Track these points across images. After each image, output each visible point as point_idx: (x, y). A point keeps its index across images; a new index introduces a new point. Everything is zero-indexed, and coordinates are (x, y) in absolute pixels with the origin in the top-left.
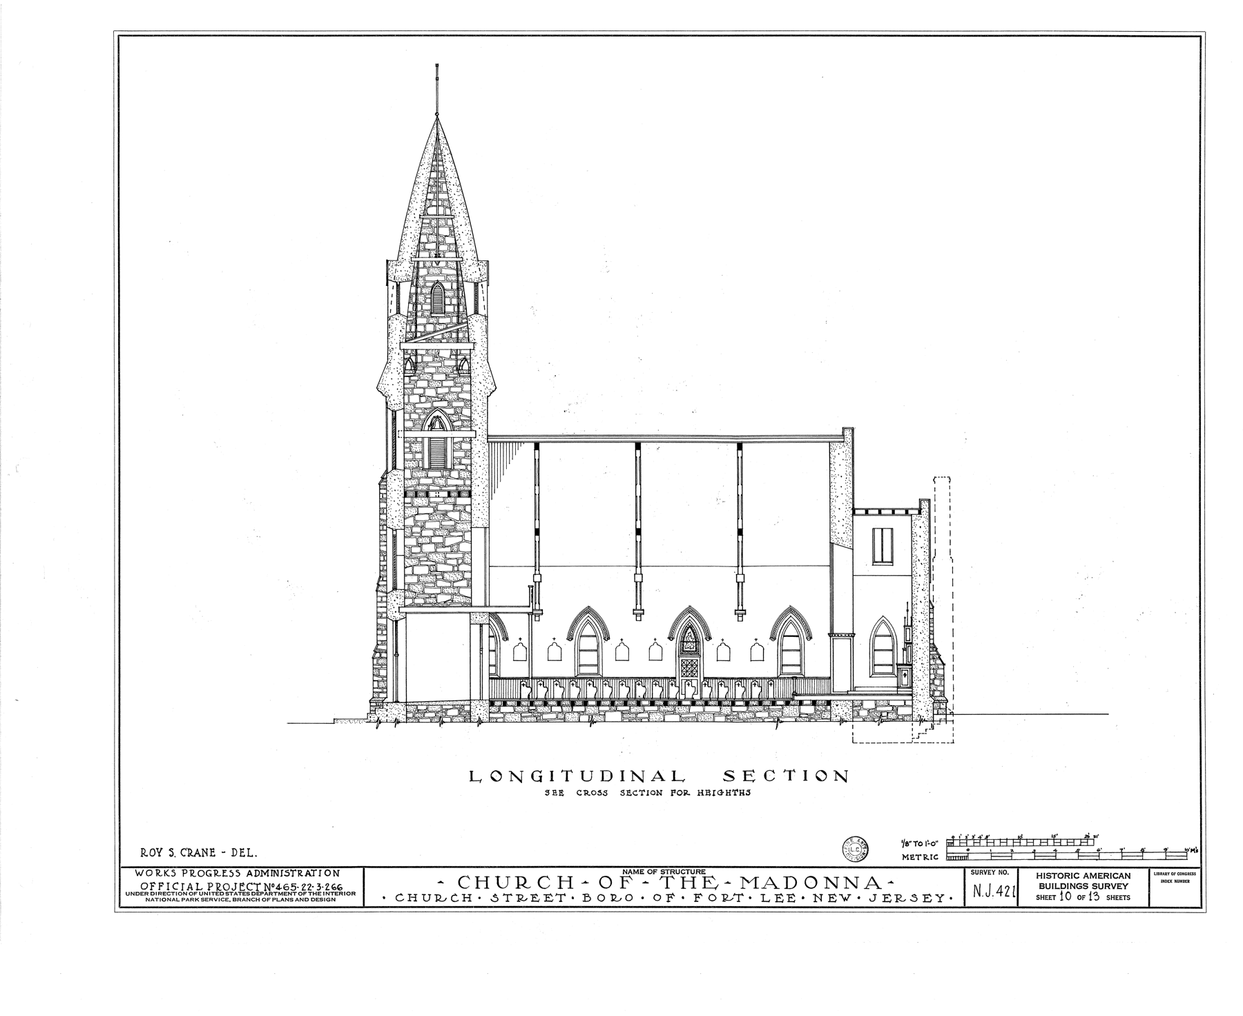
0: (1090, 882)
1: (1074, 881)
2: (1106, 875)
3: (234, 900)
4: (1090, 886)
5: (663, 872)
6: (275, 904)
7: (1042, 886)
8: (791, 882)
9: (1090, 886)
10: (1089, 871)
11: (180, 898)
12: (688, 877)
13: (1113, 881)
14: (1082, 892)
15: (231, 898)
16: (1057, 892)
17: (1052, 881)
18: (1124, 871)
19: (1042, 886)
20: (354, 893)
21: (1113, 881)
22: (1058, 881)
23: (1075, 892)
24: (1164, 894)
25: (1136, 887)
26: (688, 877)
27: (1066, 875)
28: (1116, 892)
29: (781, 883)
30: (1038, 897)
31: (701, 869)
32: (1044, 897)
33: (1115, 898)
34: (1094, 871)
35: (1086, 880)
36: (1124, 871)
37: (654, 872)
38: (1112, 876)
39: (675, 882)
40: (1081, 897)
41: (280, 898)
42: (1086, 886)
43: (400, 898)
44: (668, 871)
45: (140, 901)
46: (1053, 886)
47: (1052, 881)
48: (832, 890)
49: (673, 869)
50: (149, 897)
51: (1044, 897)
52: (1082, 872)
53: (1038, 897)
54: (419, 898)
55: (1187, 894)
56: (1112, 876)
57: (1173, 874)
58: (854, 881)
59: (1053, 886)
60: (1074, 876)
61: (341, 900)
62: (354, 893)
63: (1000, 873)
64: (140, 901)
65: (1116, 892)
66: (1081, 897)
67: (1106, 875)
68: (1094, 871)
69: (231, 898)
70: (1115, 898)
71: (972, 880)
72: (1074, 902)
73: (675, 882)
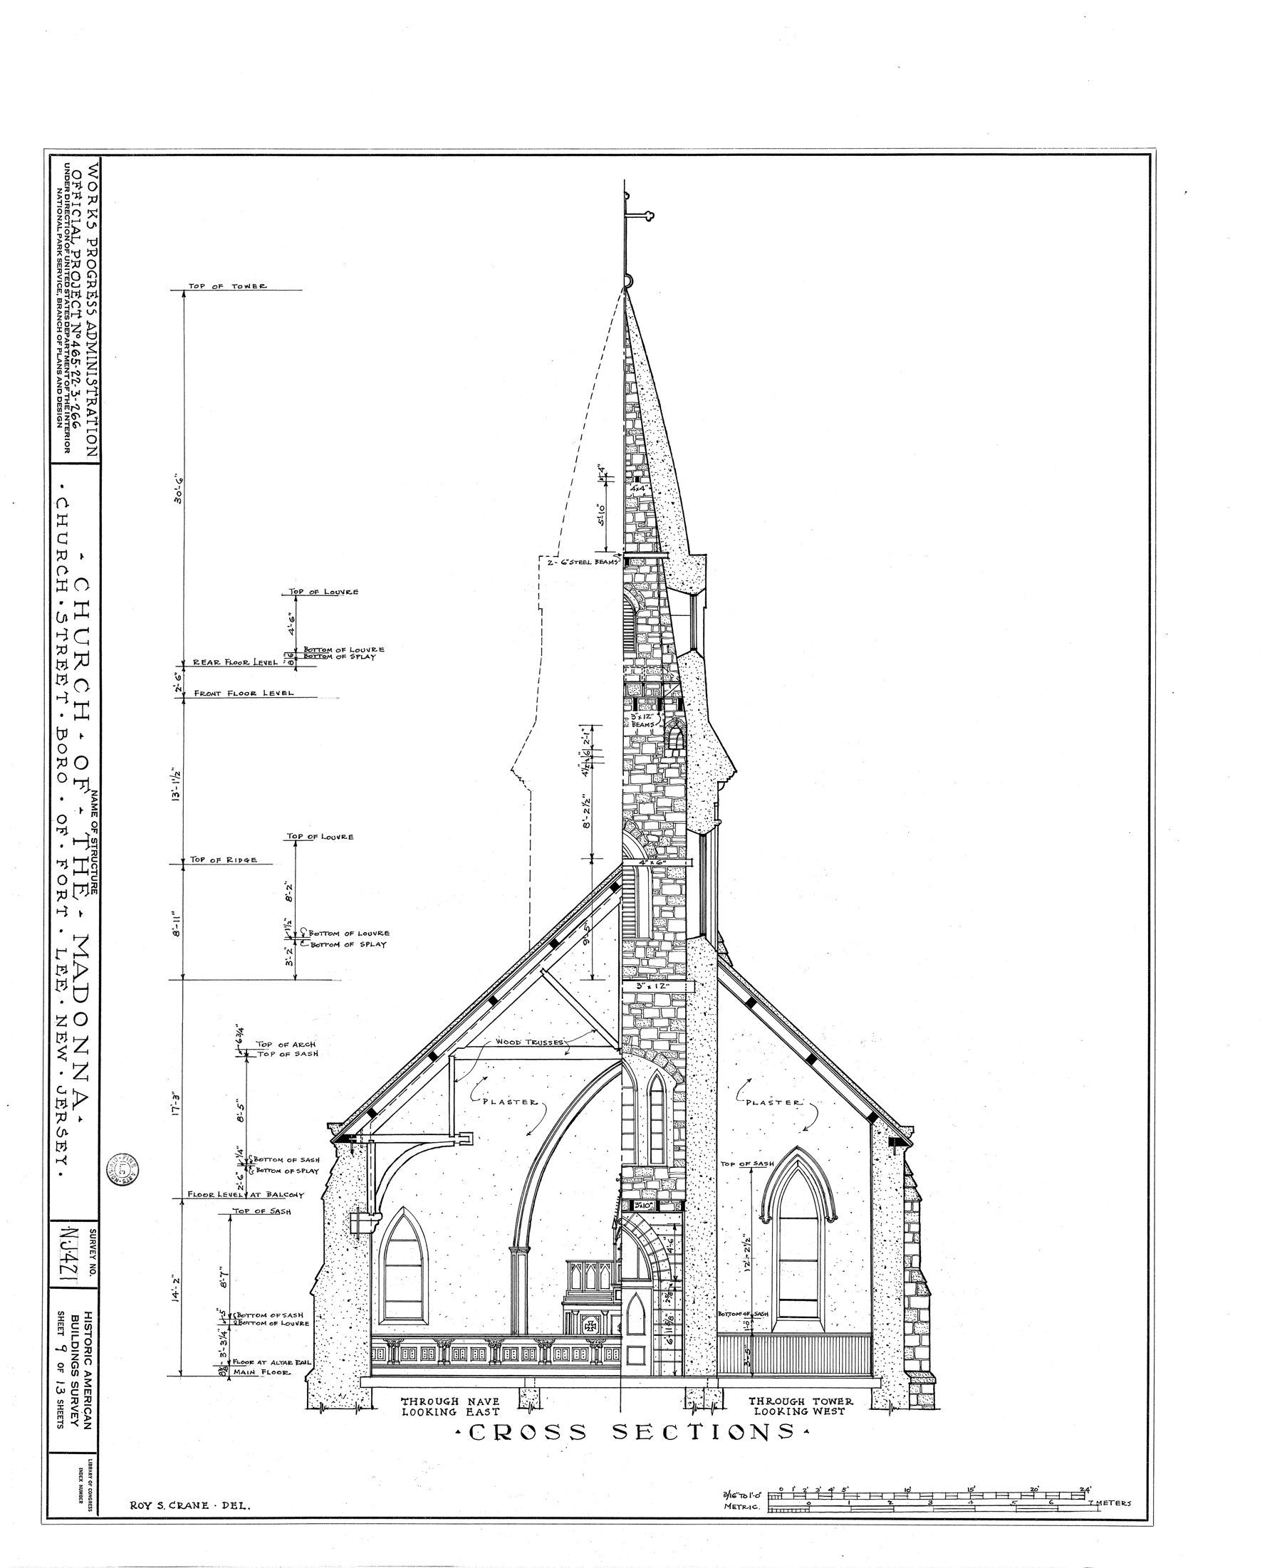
0: (81, 1379)
1: (81, 1358)
2: (88, 1399)
3: (60, 300)
4: (75, 1379)
5: (94, 840)
6: (54, 352)
7: (75, 1318)
8: (81, 995)
9: (75, 1379)
10: (94, 1377)
11: (62, 231)
12: (87, 866)
13: (81, 1407)
14: (68, 1368)
15: (62, 295)
16: (66, 1339)
17: (82, 1331)
18: (94, 1421)
19: (75, 1318)
20: (68, 451)
21: (81, 1407)
22: (81, 1338)
23: (67, 1358)
24: (66, 1471)
25: (72, 1437)
26: (87, 866)
27: (89, 1350)
28: (67, 1411)
29: (80, 982)
30: (61, 1314)
31: (97, 888)
32: (61, 1321)
33: (60, 1410)
34: (94, 1383)
35: (82, 1374)
36: (94, 1421)
37: (95, 830)
38: (88, 1407)
39: (82, 851)
40: (61, 1367)
41: (62, 357)
42: (75, 1373)
43: (62, 503)
44: (97, 846)
45: (58, 182)
46: (75, 1333)
47: (82, 1331)
48: (72, 1046)
49: (98, 853)
50: (64, 193)
51: (61, 1321)
52: (93, 1369)
53: (61, 1314)
54: (63, 529)
55: (66, 1501)
56: (88, 1407)
57: (90, 1483)
58: (83, 1075)
59: (75, 1333)
60: (88, 1358)
61: (58, 434)
62: (68, 451)
63: (93, 1266)
64: (58, 182)
65: (67, 1411)
66: (61, 1367)
67: (88, 1399)
68: (94, 1383)
69: (62, 295)
70: (60, 1410)
71: (85, 1229)
72: (56, 1357)
73: (82, 851)
